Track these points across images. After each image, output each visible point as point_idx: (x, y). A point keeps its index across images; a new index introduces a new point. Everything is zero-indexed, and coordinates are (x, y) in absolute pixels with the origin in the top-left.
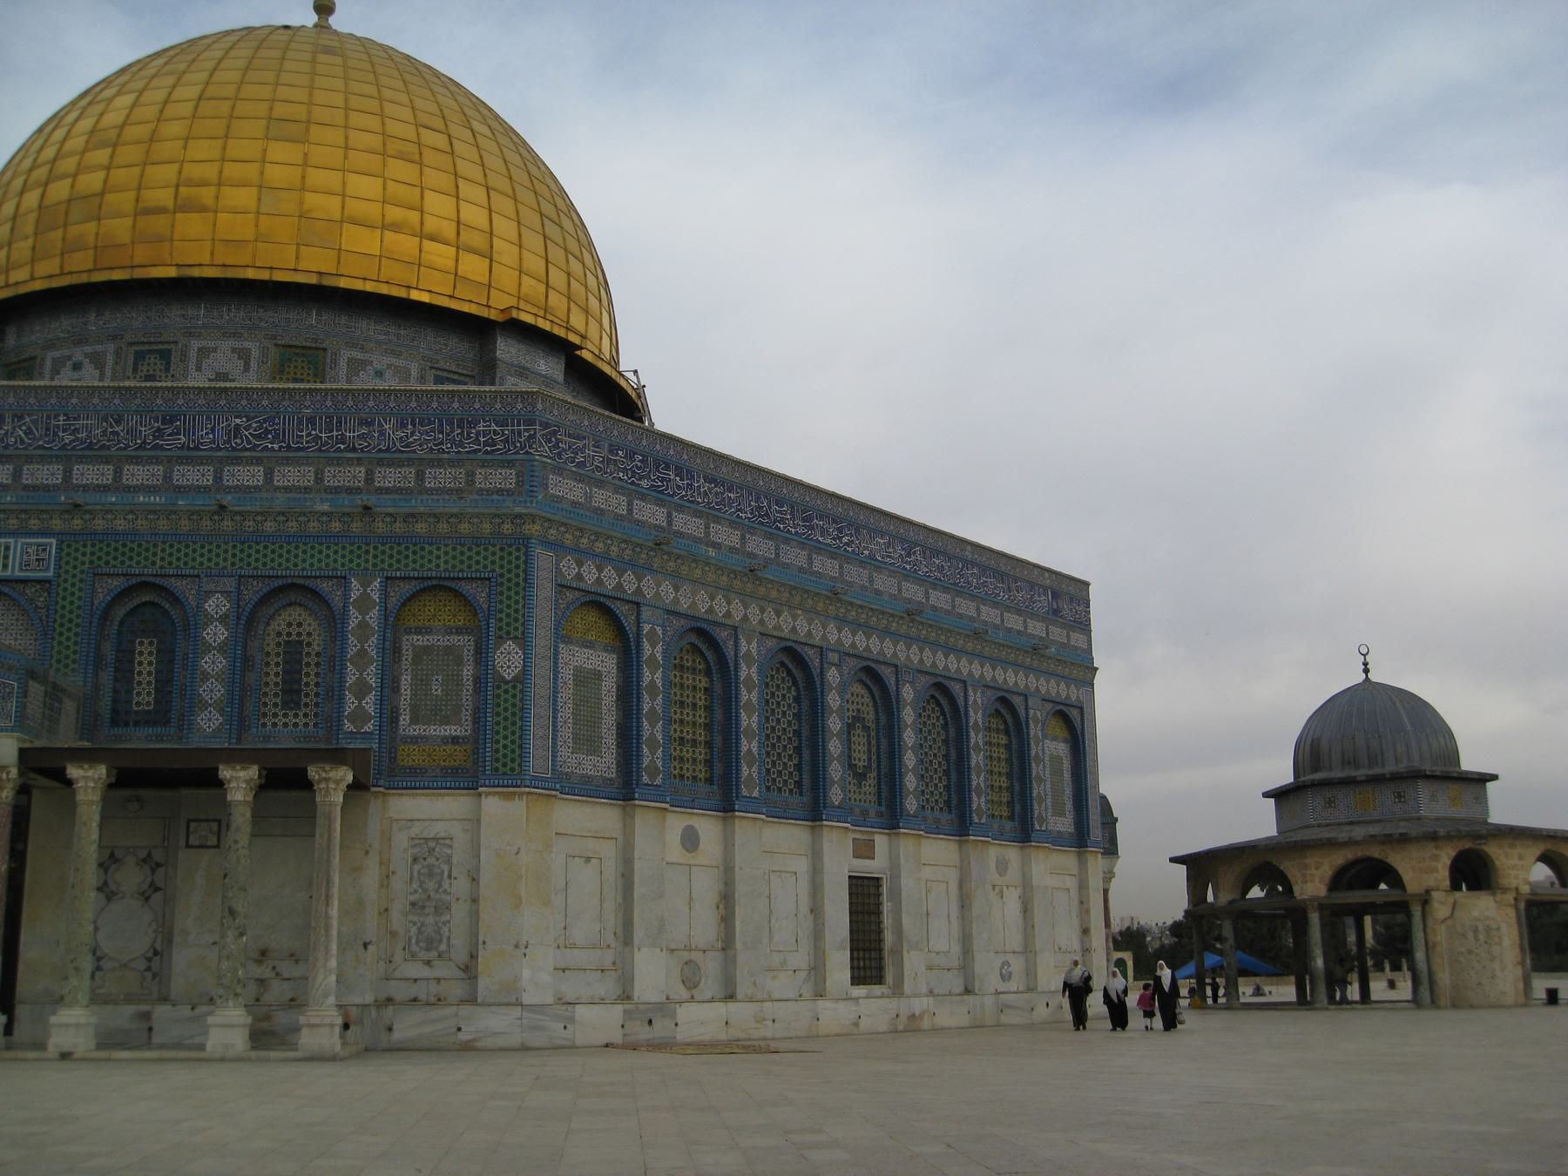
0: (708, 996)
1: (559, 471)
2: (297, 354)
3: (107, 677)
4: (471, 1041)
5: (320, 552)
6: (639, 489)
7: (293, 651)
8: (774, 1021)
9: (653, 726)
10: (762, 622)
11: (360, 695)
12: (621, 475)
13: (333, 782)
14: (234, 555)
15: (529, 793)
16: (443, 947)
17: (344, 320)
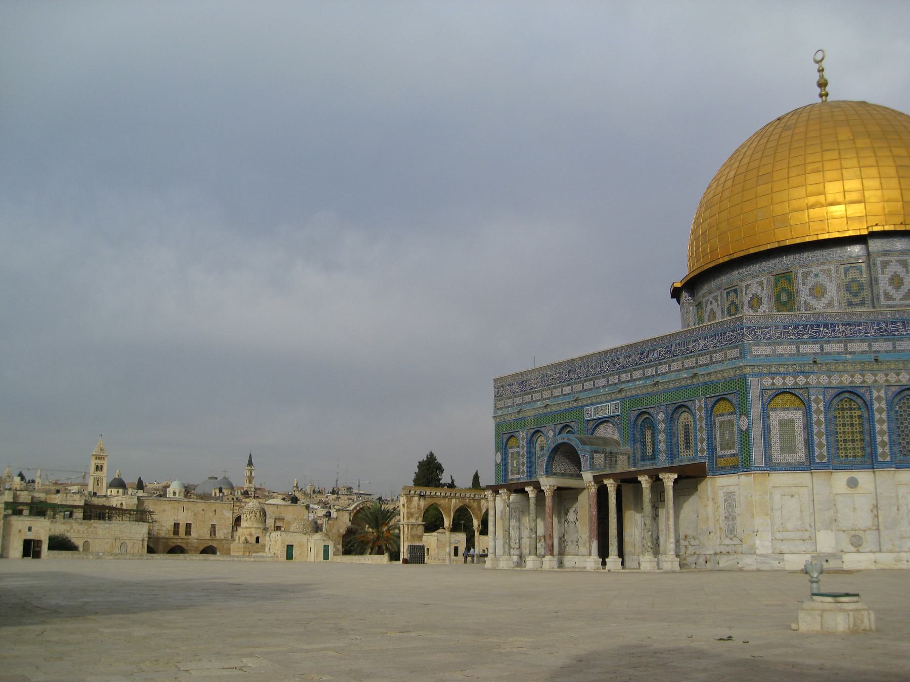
0: (869, 549)
1: (758, 344)
2: (781, 277)
3: (638, 445)
4: (742, 567)
5: (686, 392)
6: (802, 340)
7: (687, 427)
8: (907, 561)
9: (820, 438)
10: (887, 381)
11: (702, 443)
12: (791, 337)
13: (669, 480)
14: (664, 398)
15: (754, 473)
16: (735, 533)
17: (797, 256)
